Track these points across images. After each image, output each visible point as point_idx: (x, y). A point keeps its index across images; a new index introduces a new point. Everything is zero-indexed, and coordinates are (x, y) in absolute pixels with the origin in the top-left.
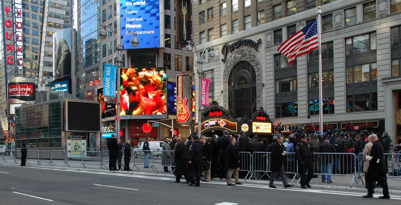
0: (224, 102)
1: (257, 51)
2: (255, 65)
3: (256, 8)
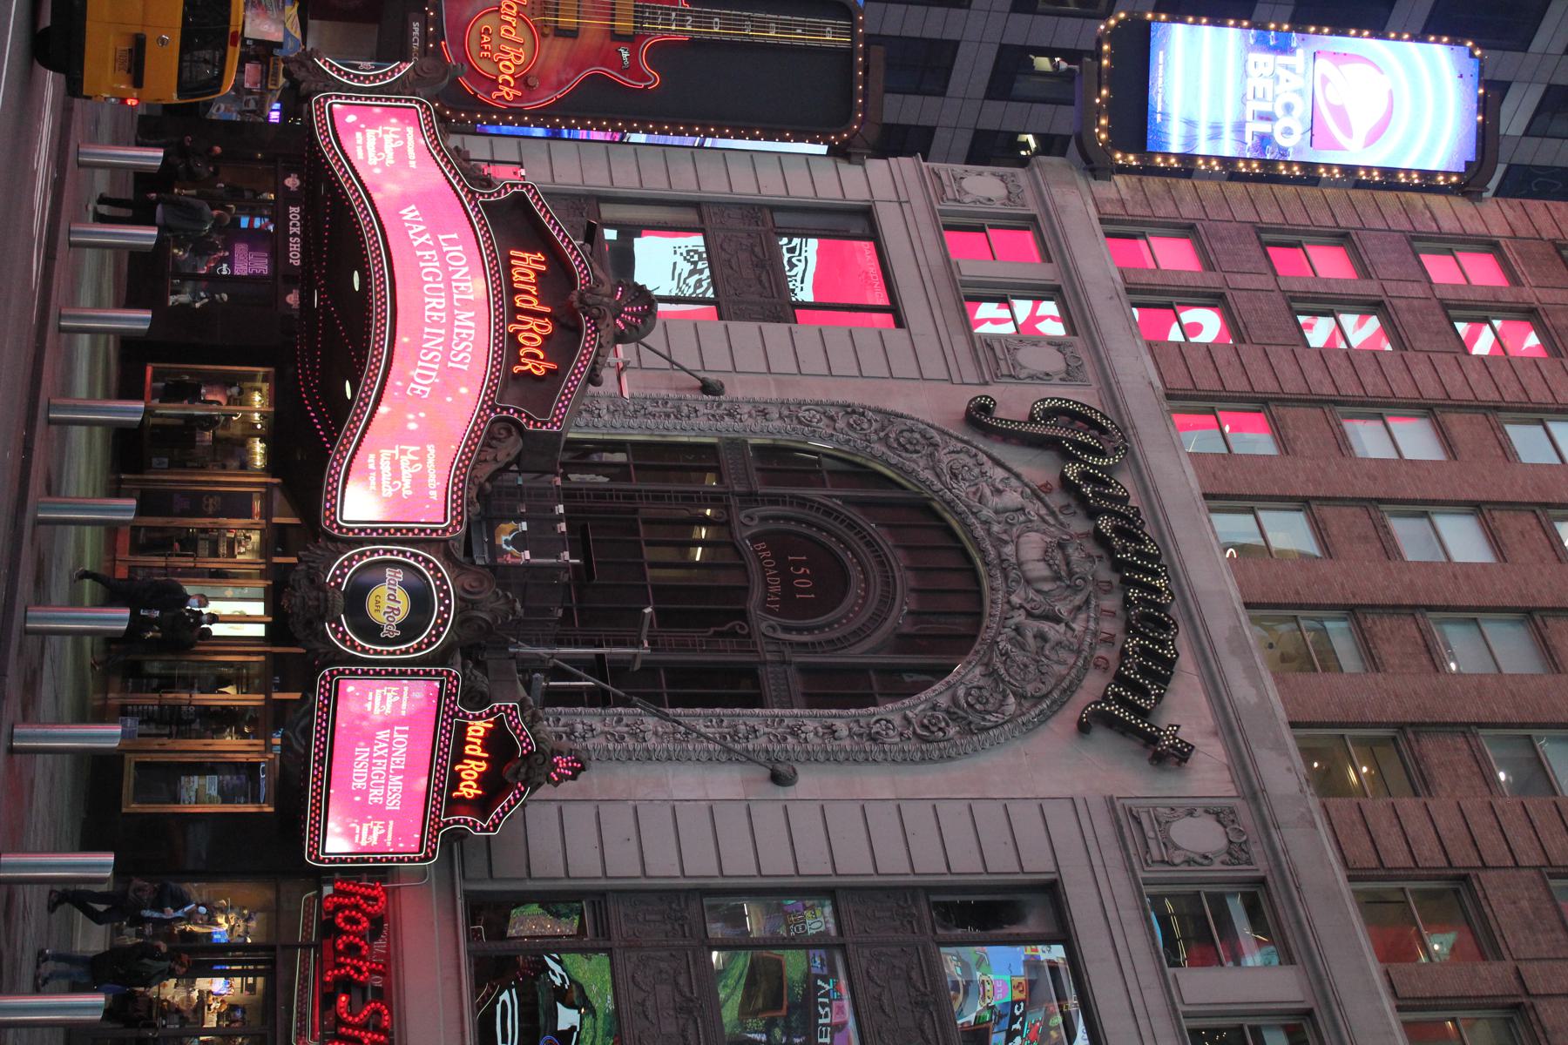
0: (640, 408)
1: (1083, 728)
2: (955, 700)
3: (1437, 719)
